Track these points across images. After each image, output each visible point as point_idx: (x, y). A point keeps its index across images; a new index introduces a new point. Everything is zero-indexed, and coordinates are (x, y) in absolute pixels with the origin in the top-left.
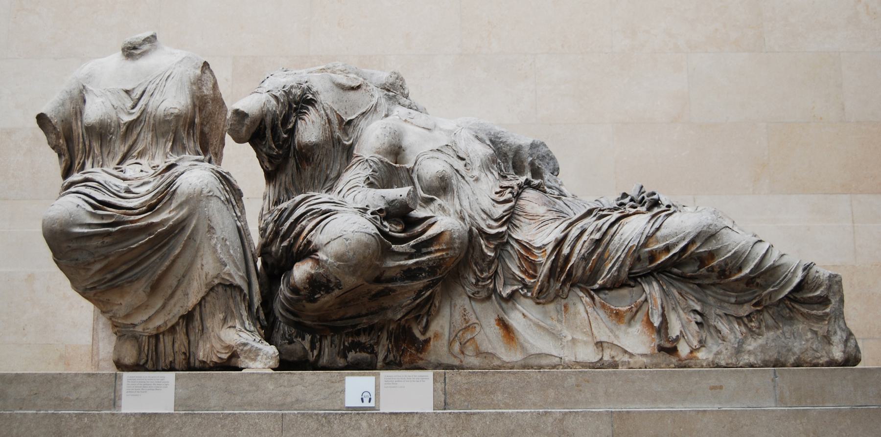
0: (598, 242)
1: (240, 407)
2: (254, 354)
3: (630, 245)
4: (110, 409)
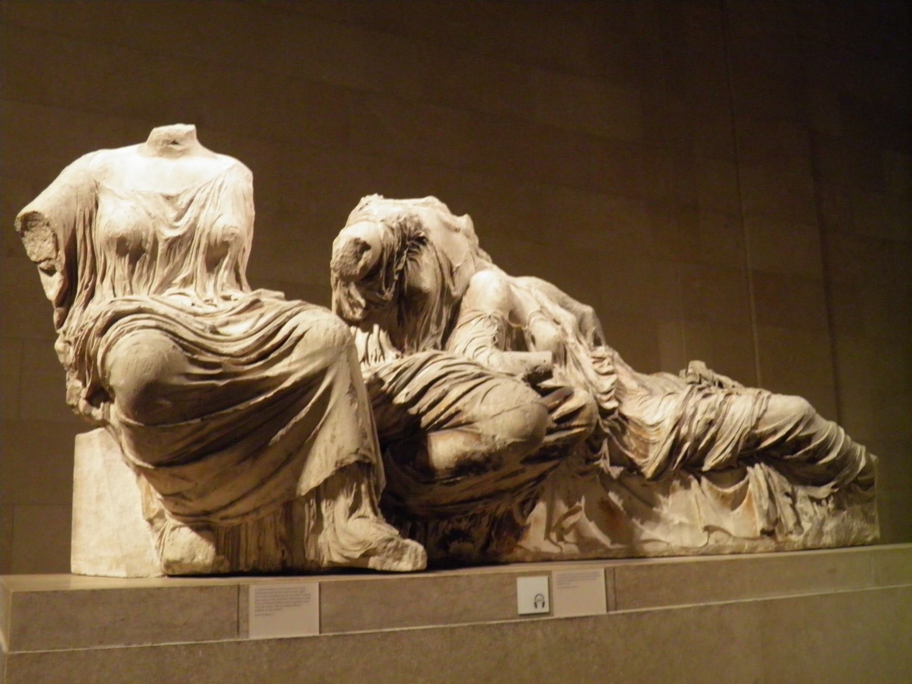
0: (710, 423)
1: (400, 623)
2: (399, 552)
3: (744, 426)
4: (232, 636)
